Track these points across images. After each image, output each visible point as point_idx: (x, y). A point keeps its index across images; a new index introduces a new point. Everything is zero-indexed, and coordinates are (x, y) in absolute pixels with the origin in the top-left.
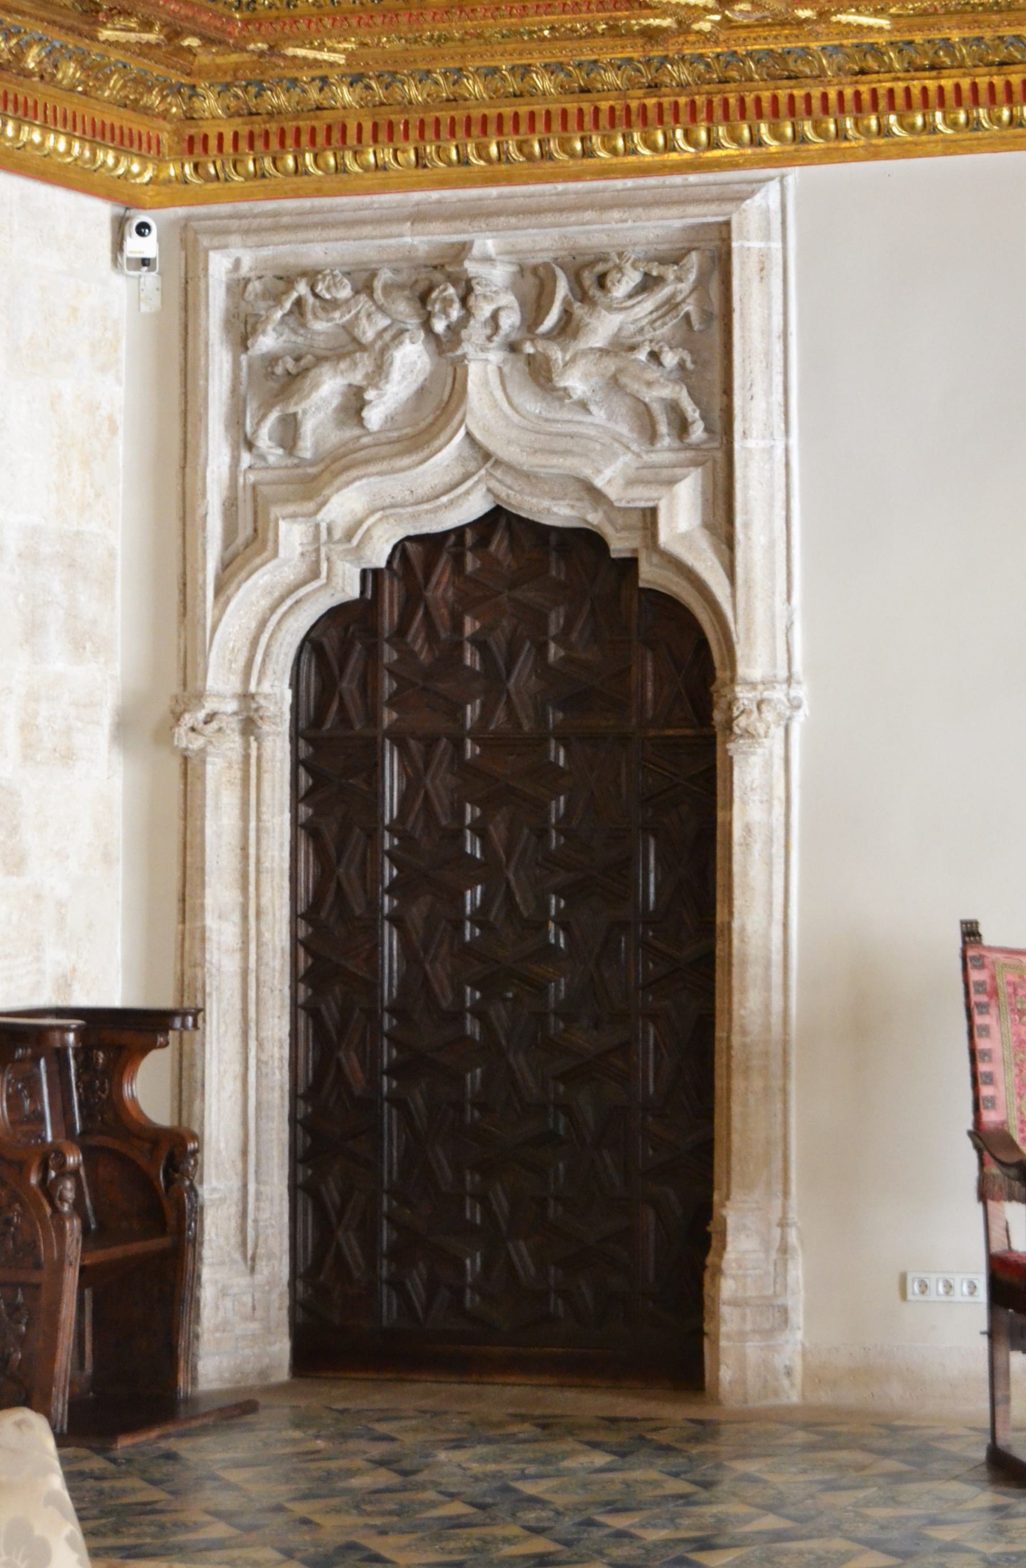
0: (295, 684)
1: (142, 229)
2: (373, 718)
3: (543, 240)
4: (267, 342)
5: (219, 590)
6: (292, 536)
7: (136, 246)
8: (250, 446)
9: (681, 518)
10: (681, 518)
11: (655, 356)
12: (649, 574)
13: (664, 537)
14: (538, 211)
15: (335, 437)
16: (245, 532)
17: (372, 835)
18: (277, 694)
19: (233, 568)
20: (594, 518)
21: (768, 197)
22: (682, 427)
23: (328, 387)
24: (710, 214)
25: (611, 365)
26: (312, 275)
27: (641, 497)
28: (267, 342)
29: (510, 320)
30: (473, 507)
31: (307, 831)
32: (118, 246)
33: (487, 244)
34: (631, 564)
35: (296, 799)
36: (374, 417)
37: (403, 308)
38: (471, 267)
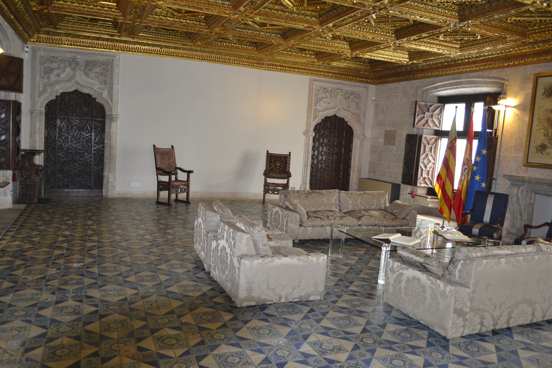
0: (45, 109)
1: (28, 47)
2: (56, 114)
3: (86, 58)
4: (46, 65)
5: (39, 96)
6: (49, 90)
7: (26, 49)
8: (43, 78)
9: (105, 94)
10: (105, 94)
11: (102, 74)
12: (98, 100)
13: (103, 96)
14: (87, 54)
15: (55, 79)
16: (41, 89)
17: (55, 129)
18: (43, 110)
19: (40, 94)
20: (91, 93)
21: (118, 57)
22: (105, 84)
23: (56, 72)
24: (111, 58)
25: (97, 75)
26: (54, 57)
27: (100, 91)
28: (46, 65)
29: (82, 68)
30: (74, 89)
31: (46, 128)
32: (23, 49)
33: (78, 57)
34: (95, 99)
35: (45, 123)
36: (62, 76)
37: (67, 63)
38: (77, 60)
